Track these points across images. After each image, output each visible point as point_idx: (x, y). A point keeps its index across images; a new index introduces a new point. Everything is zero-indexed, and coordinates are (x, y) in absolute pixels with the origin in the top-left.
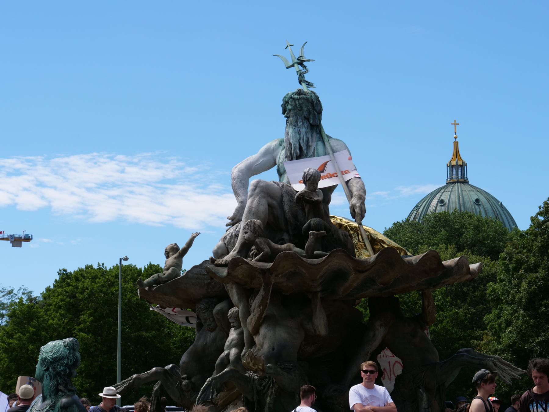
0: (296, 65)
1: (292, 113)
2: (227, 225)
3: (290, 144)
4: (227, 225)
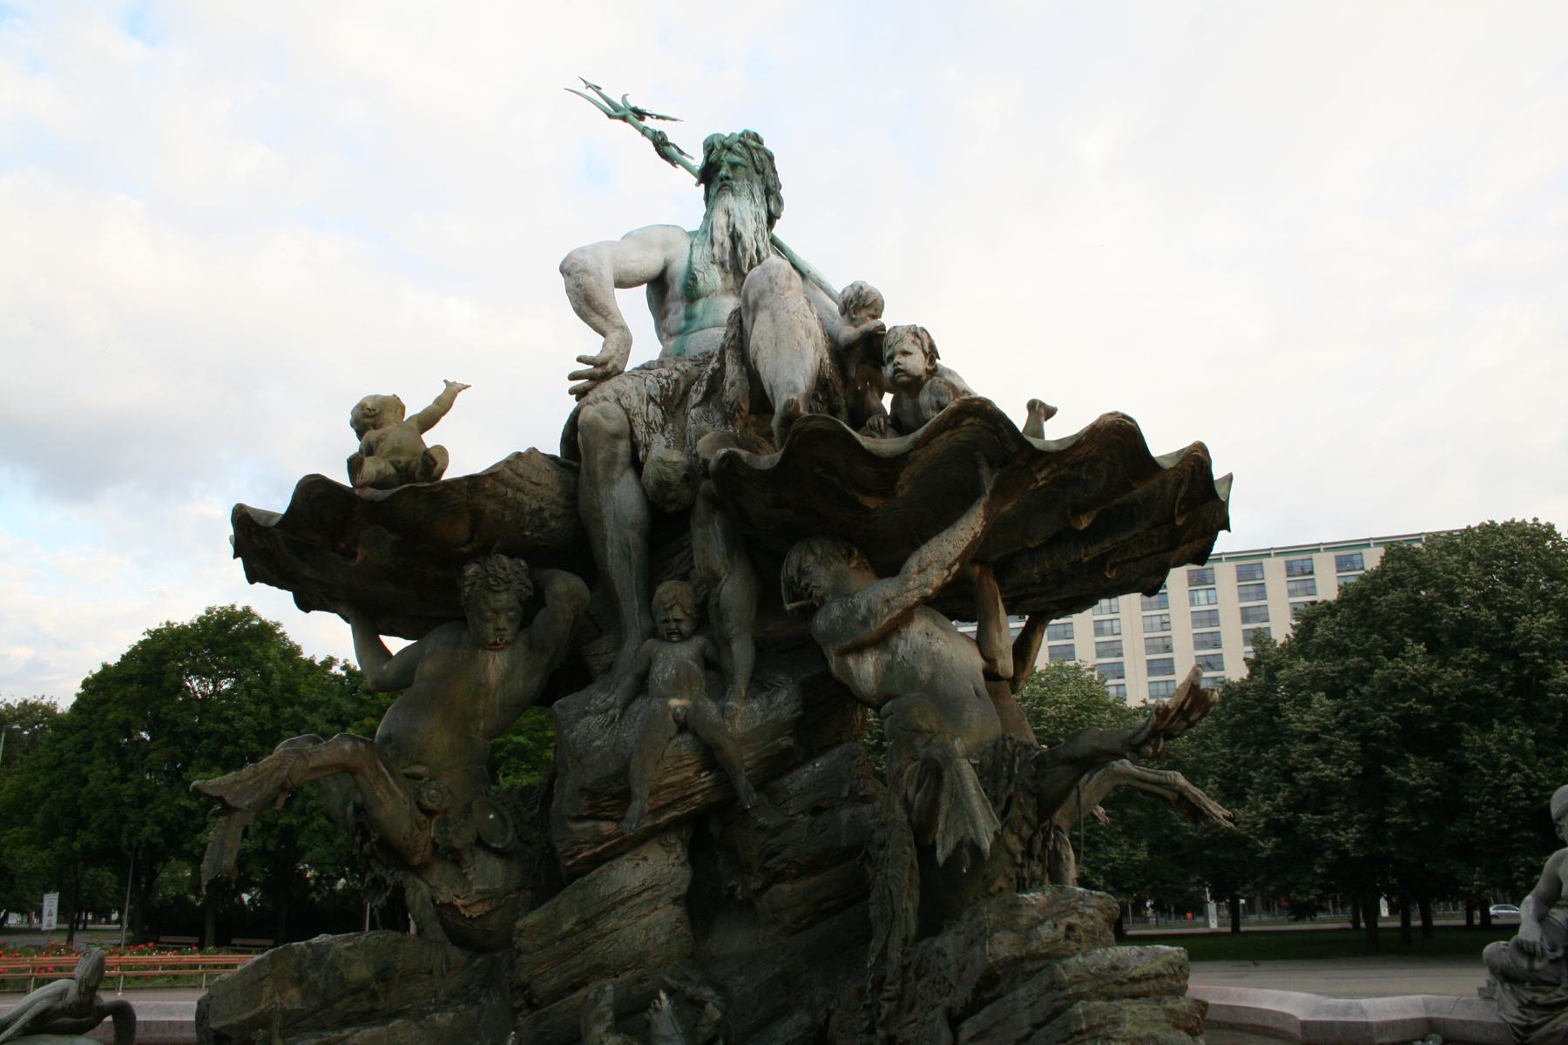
0: (631, 117)
1: (741, 170)
2: (573, 377)
3: (735, 238)
4: (573, 377)
